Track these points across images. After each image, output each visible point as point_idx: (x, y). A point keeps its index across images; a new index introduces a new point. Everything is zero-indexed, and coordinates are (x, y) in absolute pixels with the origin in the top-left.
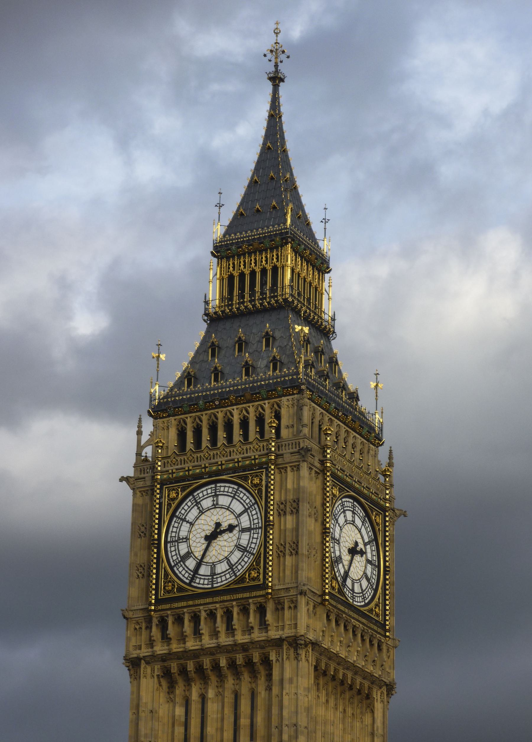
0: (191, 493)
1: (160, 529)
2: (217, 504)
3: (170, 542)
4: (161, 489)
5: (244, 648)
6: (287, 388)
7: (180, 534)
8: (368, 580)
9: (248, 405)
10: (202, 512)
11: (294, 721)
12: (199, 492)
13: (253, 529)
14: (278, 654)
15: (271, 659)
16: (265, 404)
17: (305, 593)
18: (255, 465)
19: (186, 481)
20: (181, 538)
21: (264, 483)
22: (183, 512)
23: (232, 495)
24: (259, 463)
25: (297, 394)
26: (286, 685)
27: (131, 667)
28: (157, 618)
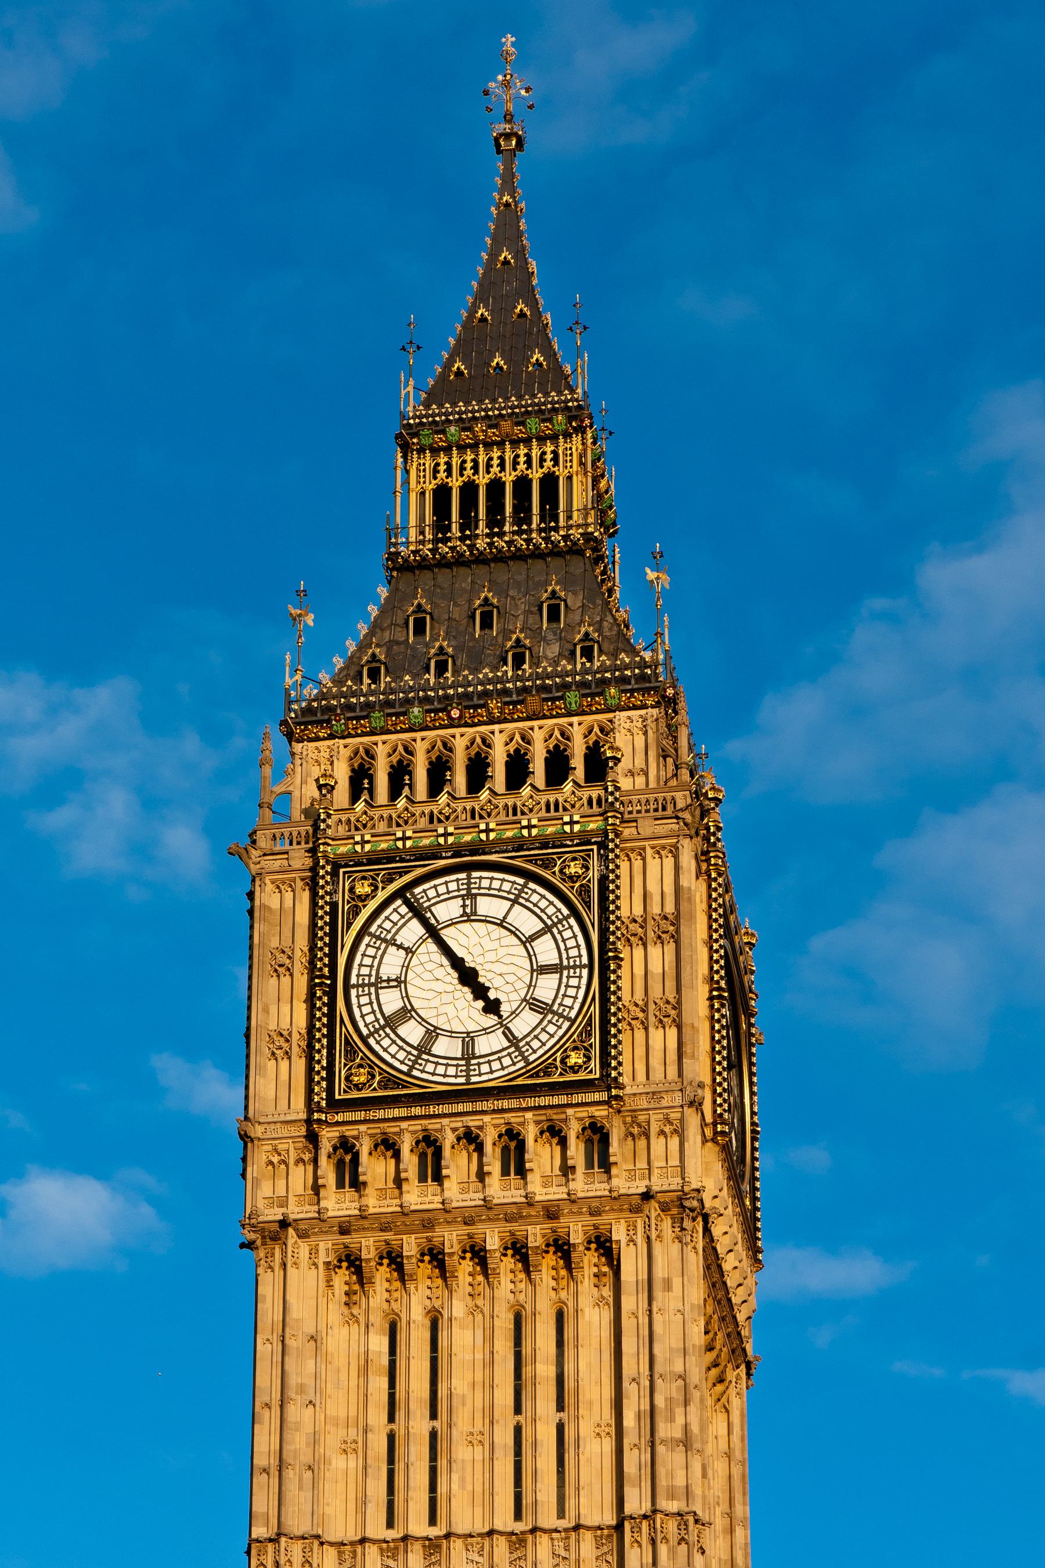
1: (333, 957)
3: (357, 986)
4: (334, 874)
5: (551, 1213)
6: (632, 691)
9: (529, 724)
11: (679, 1368)
12: (426, 886)
13: (568, 968)
14: (631, 1227)
16: (571, 725)
17: (701, 1104)
18: (572, 836)
19: (397, 862)
20: (385, 978)
21: (594, 874)
22: (388, 925)
23: (512, 897)
24: (580, 831)
25: (653, 707)
26: (658, 1293)
28: (329, 1140)
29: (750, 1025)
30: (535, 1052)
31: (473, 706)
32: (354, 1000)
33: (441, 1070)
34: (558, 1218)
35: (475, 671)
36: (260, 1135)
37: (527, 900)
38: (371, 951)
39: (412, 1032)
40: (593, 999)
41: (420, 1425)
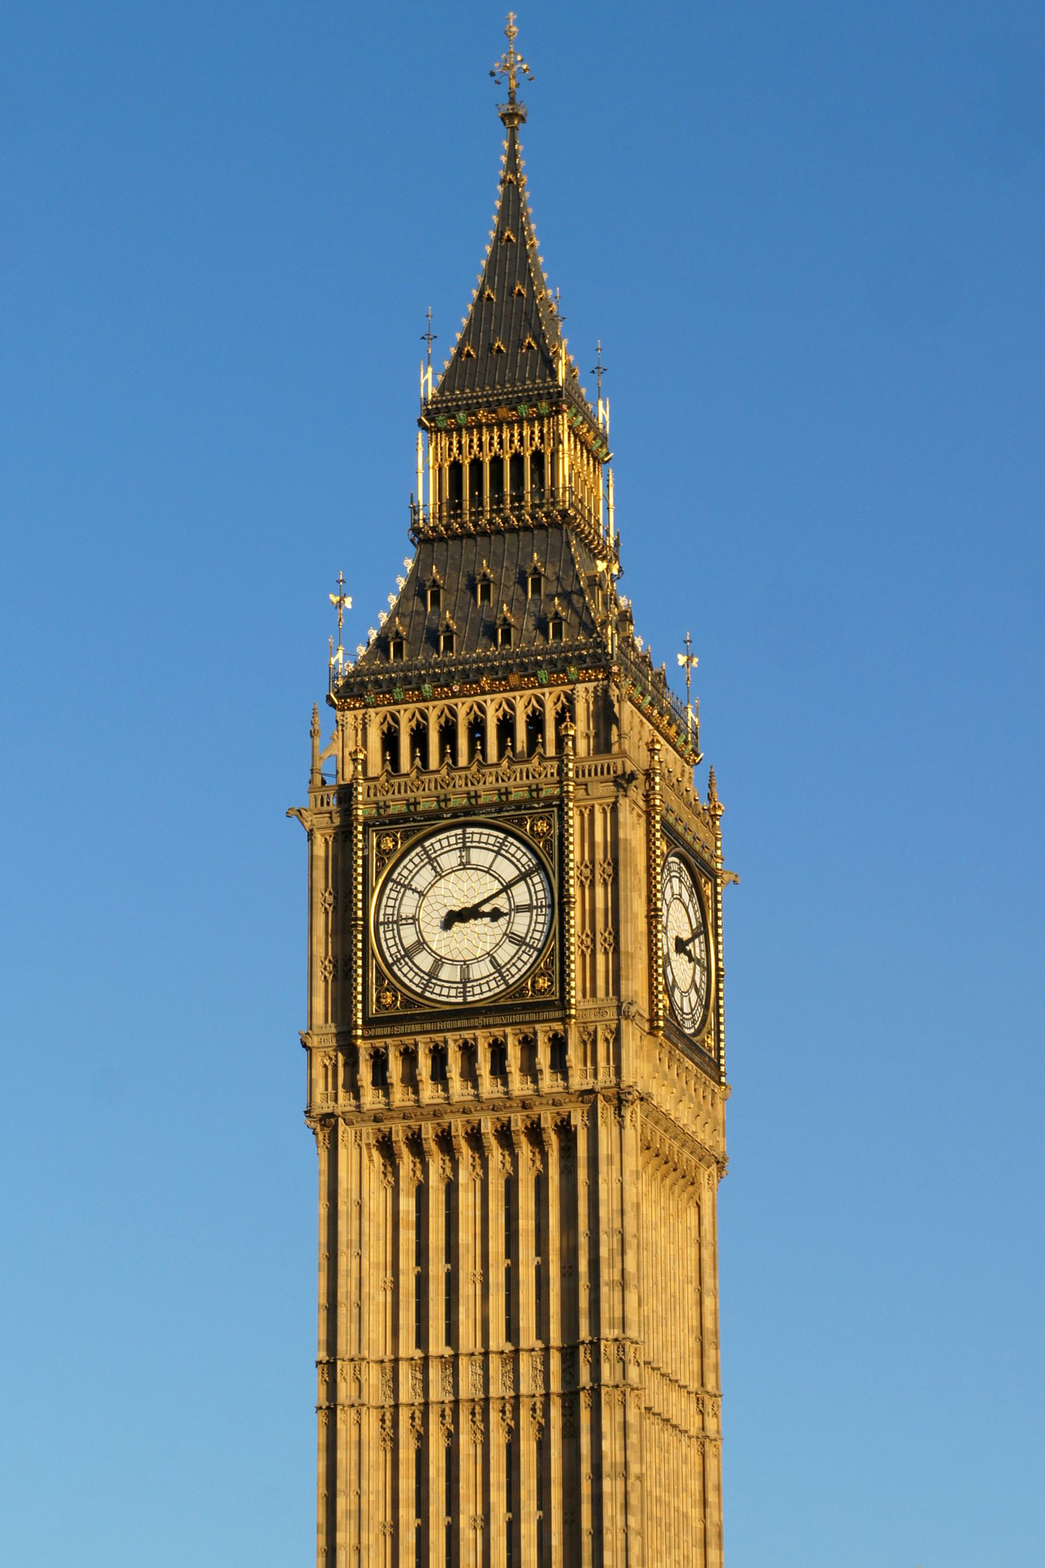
0: (420, 842)
2: (469, 863)
3: (383, 923)
7: (402, 911)
8: (697, 991)
10: (440, 875)
12: (433, 840)
13: (537, 907)
15: (573, 1122)
23: (496, 849)
27: (318, 1130)
29: (716, 885)
30: (513, 976)
31: (469, 678)
32: (382, 935)
33: (445, 992)
34: (531, 1108)
35: (471, 649)
36: (316, 1044)
37: (507, 851)
38: (394, 895)
39: (424, 960)
40: (554, 935)
41: (438, 1268)
